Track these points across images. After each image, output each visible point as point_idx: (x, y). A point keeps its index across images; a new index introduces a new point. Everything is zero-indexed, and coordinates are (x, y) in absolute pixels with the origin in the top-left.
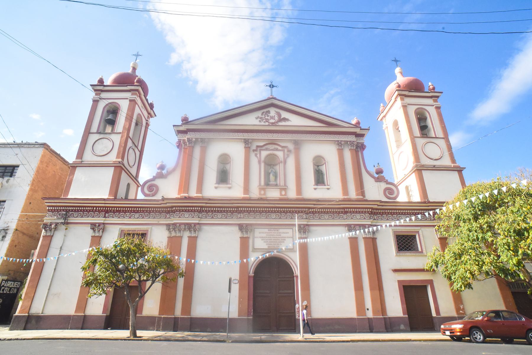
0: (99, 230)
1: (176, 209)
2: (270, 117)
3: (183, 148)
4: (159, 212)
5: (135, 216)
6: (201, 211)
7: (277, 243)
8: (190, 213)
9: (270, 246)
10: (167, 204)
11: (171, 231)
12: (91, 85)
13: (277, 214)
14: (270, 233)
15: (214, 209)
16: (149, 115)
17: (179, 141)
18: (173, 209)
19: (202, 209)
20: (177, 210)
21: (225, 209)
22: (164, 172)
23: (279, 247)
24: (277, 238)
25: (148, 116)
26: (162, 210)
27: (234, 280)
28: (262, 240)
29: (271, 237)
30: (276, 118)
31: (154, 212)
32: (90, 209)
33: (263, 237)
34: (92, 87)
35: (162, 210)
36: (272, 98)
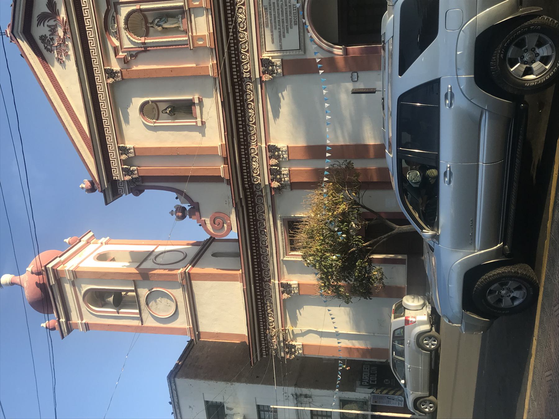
0: (289, 286)
1: (247, 182)
2: (52, 34)
3: (143, 183)
4: (254, 207)
5: (264, 240)
6: (246, 143)
7: (288, 10)
8: (251, 161)
9: (293, 20)
10: (241, 197)
11: (282, 187)
12: (63, 337)
13: (236, 11)
14: (271, 23)
15: (240, 123)
16: (92, 242)
18: (248, 188)
19: (243, 143)
20: (248, 181)
21: (239, 104)
22: (187, 206)
23: (294, 5)
24: (278, 9)
25: (93, 243)
26: (251, 204)
27: (352, 80)
28: (284, 36)
29: (279, 21)
30: (52, 23)
31: (255, 214)
32: (260, 303)
33: (280, 36)
34: (64, 335)
35: (251, 204)
36: (12, 32)
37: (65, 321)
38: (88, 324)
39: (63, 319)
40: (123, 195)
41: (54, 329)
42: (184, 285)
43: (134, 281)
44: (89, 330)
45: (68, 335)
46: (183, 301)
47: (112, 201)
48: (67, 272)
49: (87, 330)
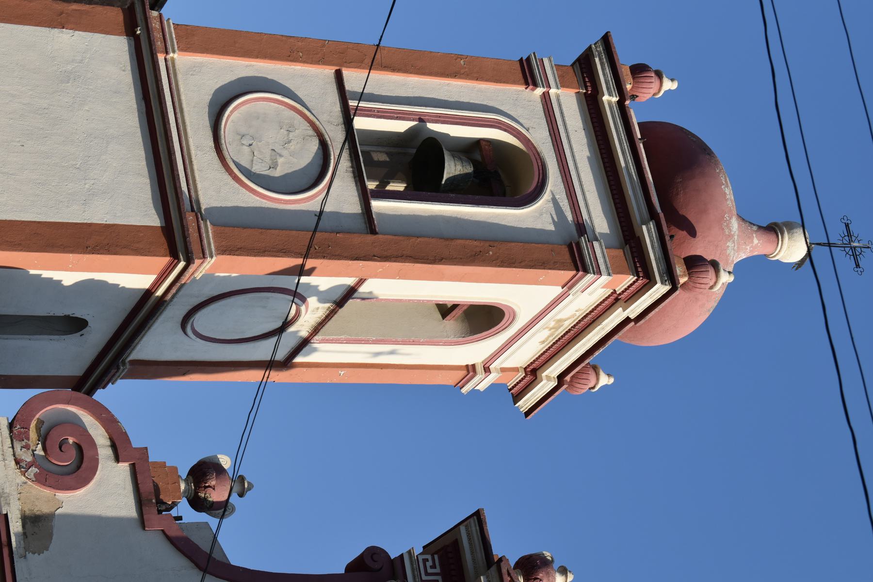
12: (606, 40)
16: (521, 374)
17: (392, 562)
25: (516, 370)
37: (604, 95)
38: (527, 84)
39: (610, 103)
40: (421, 550)
41: (638, 70)
42: (193, 210)
43: (372, 231)
44: (522, 58)
45: (590, 47)
46: (193, 152)
47: (462, 528)
48: (603, 267)
49: (528, 59)
